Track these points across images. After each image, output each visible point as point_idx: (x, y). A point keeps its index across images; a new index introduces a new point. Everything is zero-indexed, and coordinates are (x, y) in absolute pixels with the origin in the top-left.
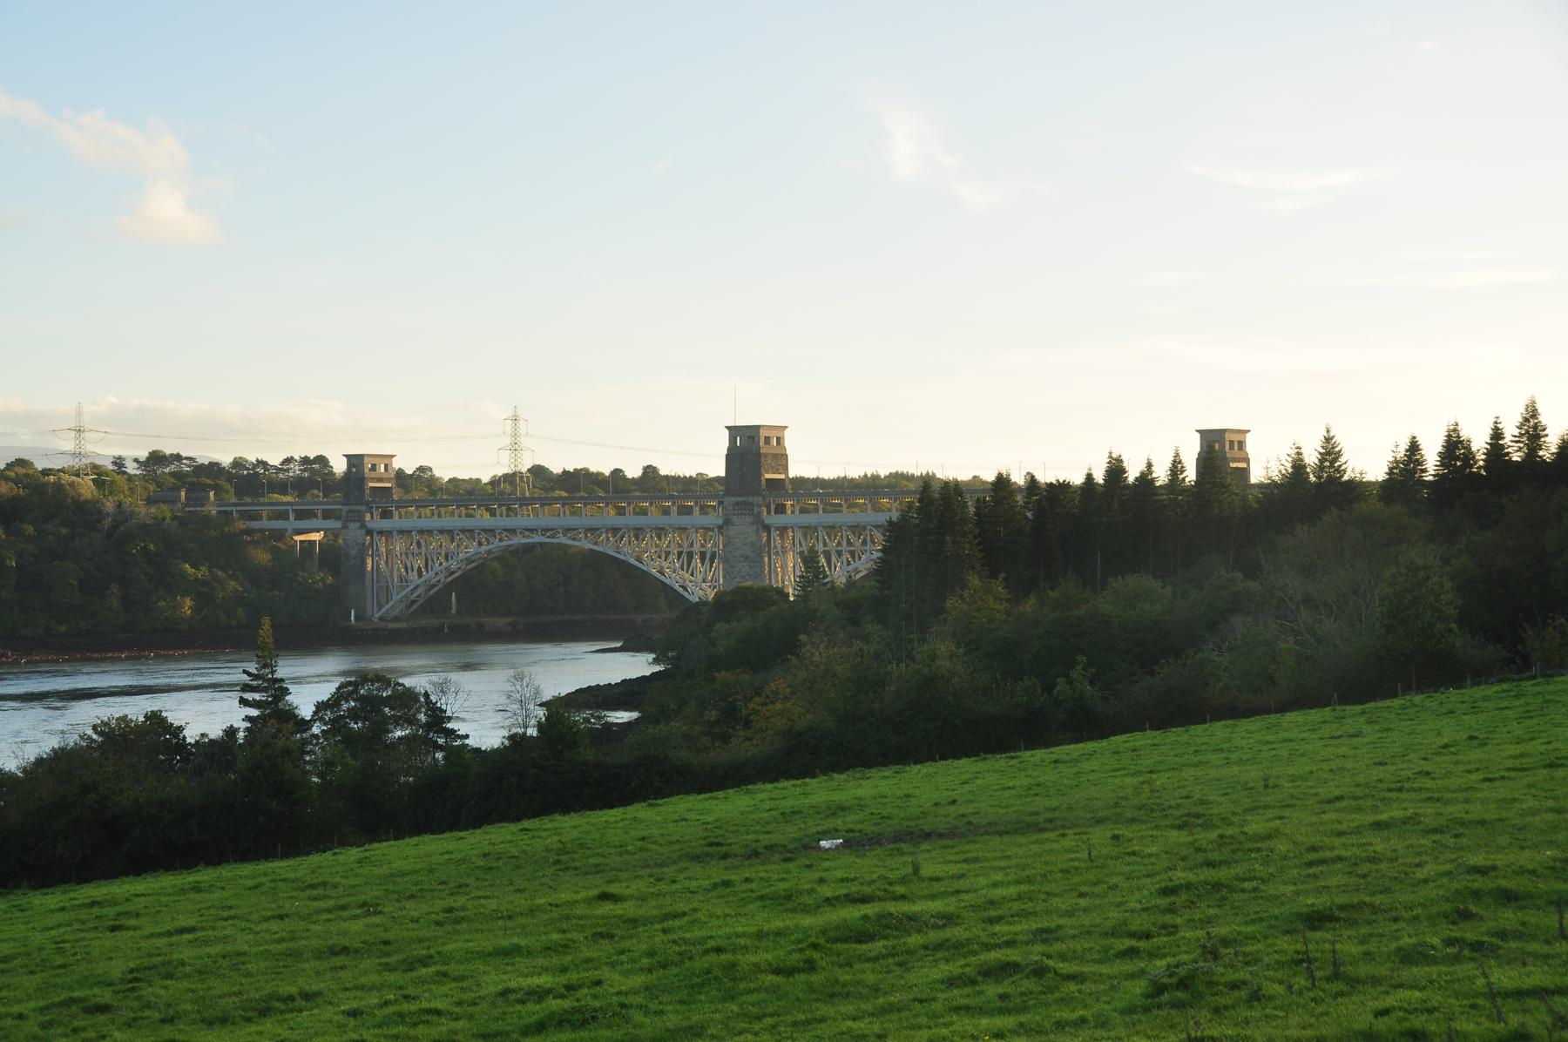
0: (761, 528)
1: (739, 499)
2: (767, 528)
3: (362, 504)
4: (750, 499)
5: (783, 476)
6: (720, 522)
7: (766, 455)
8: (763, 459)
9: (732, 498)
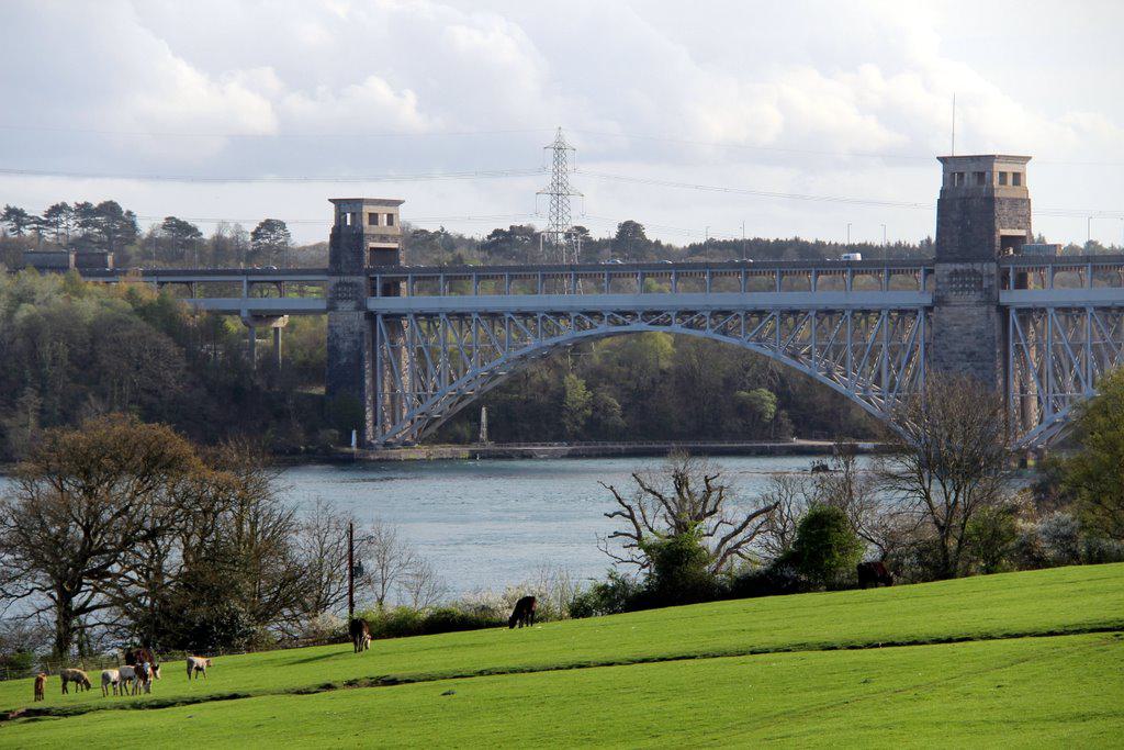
0: (993, 309)
1: (959, 267)
2: (1004, 311)
3: (359, 274)
4: (977, 267)
5: (1022, 233)
6: (928, 300)
7: (1001, 201)
8: (997, 207)
9: (948, 266)
